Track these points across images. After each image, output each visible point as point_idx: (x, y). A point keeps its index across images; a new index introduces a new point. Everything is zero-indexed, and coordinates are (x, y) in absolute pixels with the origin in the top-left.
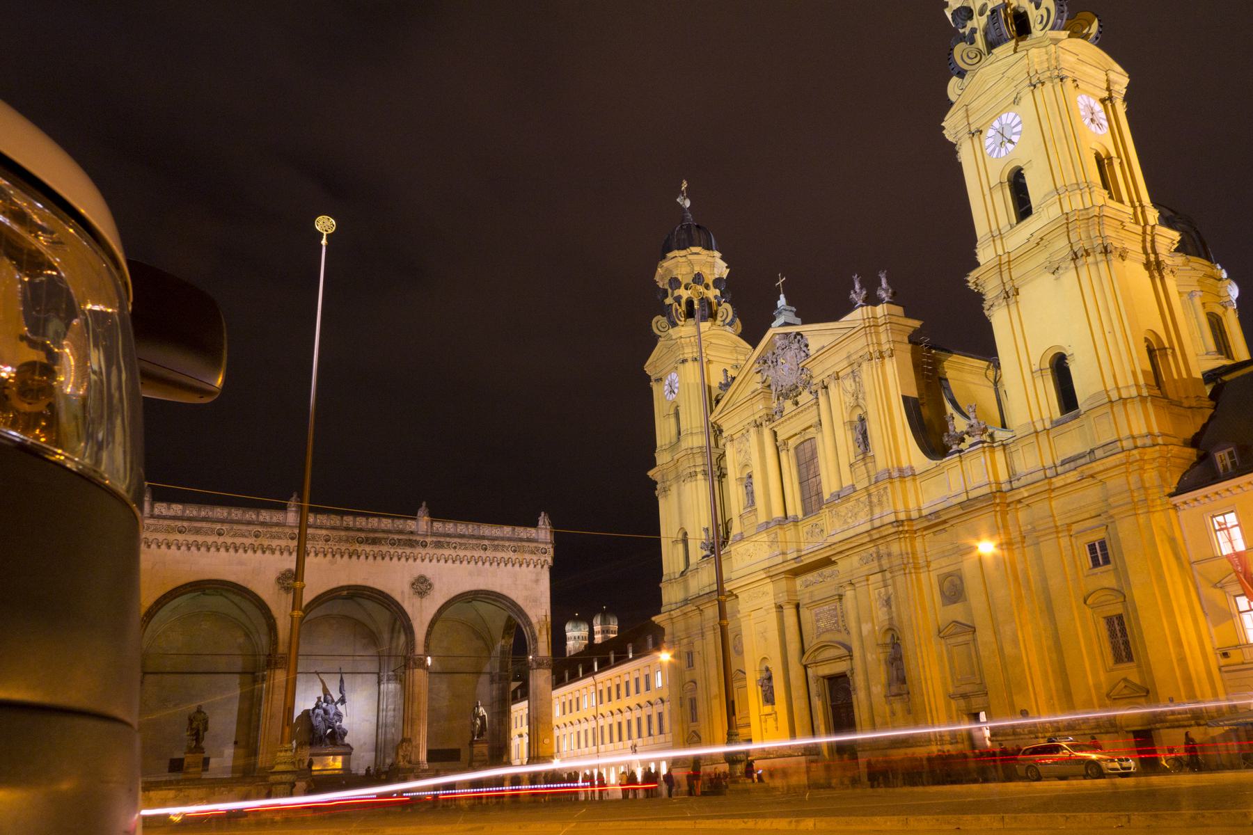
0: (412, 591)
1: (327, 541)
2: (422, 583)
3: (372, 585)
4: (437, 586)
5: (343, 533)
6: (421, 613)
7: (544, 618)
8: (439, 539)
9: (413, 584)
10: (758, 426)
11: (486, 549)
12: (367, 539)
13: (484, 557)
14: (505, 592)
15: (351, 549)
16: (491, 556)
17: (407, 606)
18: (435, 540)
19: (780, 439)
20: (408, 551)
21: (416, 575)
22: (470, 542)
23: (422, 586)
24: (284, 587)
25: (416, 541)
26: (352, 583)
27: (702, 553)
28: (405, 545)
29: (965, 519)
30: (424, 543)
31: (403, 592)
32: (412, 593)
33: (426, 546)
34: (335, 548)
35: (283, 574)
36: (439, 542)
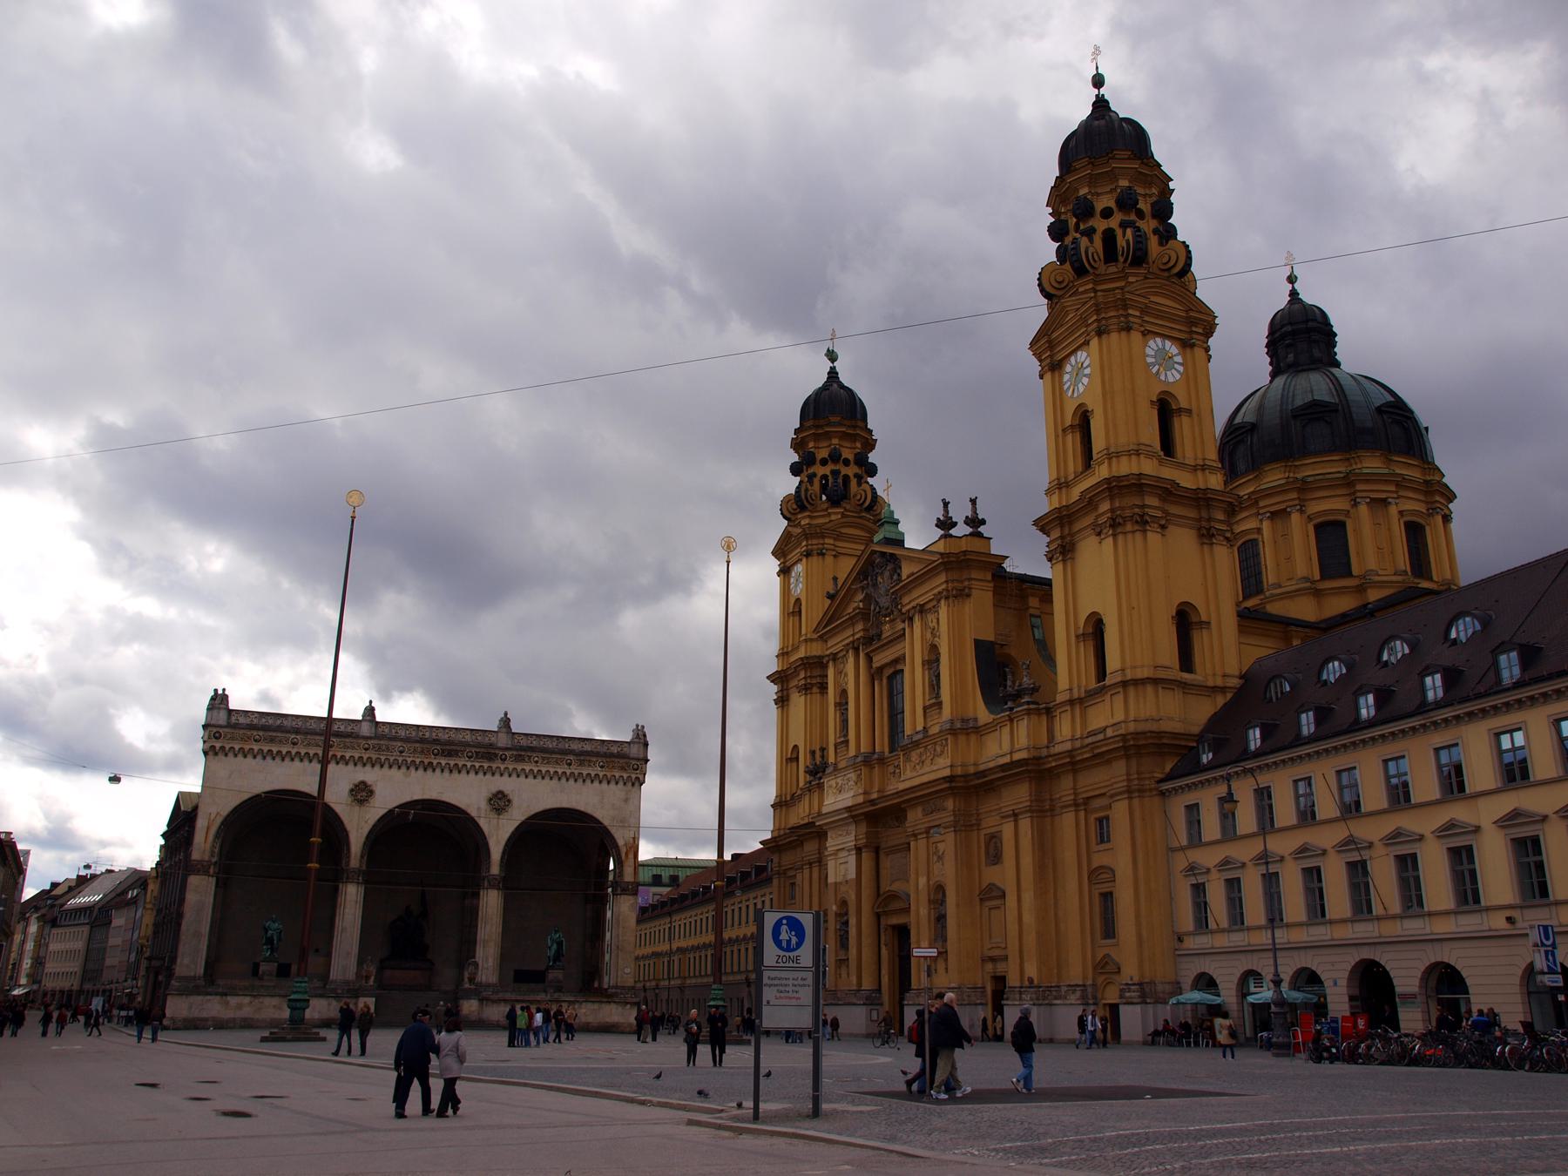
0: (488, 808)
1: (401, 752)
2: (500, 799)
3: (447, 800)
4: (515, 801)
5: (417, 745)
6: (498, 833)
7: (631, 840)
8: (520, 753)
9: (491, 799)
10: (856, 650)
11: (570, 764)
12: (443, 751)
13: (568, 772)
14: (589, 810)
15: (426, 761)
16: (576, 772)
17: (483, 823)
18: (515, 753)
19: (874, 666)
20: (486, 765)
21: (494, 790)
22: (553, 756)
23: (500, 802)
24: (358, 800)
25: (496, 755)
26: (426, 797)
27: (805, 777)
28: (482, 757)
29: (1086, 764)
30: (503, 757)
31: (479, 809)
32: (489, 810)
33: (505, 759)
34: (409, 760)
35: (356, 786)
36: (520, 755)
